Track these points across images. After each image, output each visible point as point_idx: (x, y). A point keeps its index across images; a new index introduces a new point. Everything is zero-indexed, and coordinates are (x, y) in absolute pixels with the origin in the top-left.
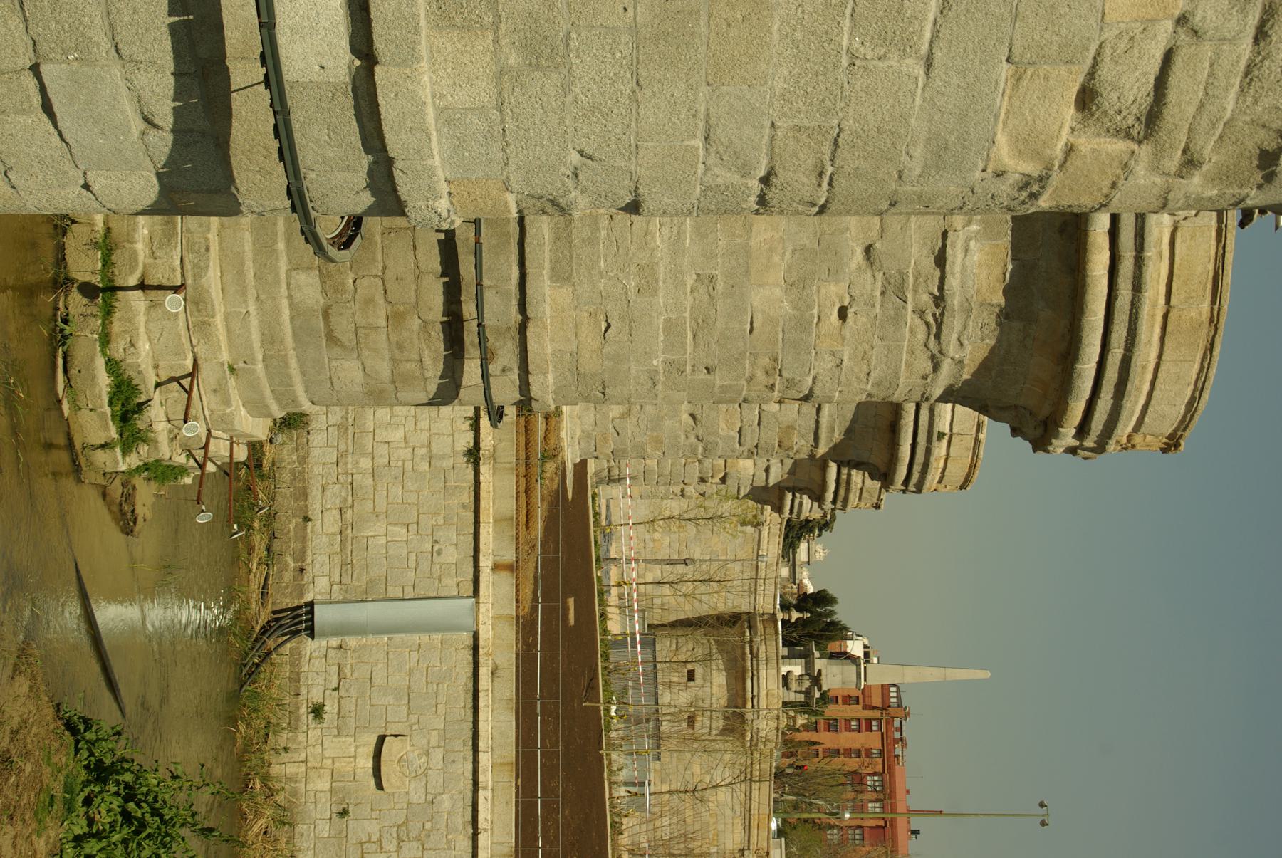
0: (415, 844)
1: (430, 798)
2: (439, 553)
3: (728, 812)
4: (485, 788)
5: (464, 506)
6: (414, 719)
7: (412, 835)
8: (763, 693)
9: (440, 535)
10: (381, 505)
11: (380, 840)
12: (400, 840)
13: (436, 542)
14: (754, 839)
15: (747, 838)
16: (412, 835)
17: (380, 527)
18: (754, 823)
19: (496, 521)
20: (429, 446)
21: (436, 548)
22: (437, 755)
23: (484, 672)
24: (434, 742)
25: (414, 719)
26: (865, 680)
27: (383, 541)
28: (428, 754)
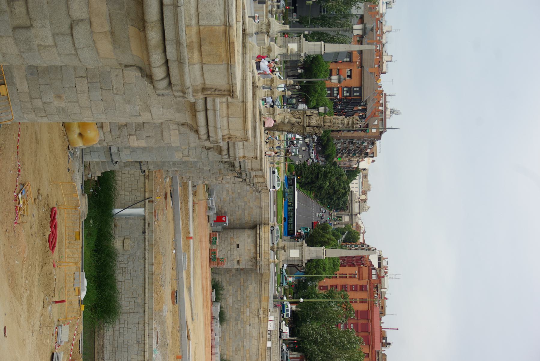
0: (132, 262)
1: (135, 252)
2: (136, 198)
3: (253, 296)
4: (147, 250)
5: (142, 188)
6: (131, 235)
7: (131, 260)
8: (263, 252)
9: (137, 194)
10: (123, 188)
11: (124, 261)
12: (128, 261)
13: (136, 196)
14: (262, 305)
15: (260, 305)
16: (131, 260)
17: (123, 192)
18: (262, 300)
19: (149, 191)
20: (134, 174)
21: (136, 197)
22: (136, 243)
23: (147, 225)
24: (135, 240)
25: (131, 235)
26: (326, 255)
27: (124, 195)
28: (134, 242)
